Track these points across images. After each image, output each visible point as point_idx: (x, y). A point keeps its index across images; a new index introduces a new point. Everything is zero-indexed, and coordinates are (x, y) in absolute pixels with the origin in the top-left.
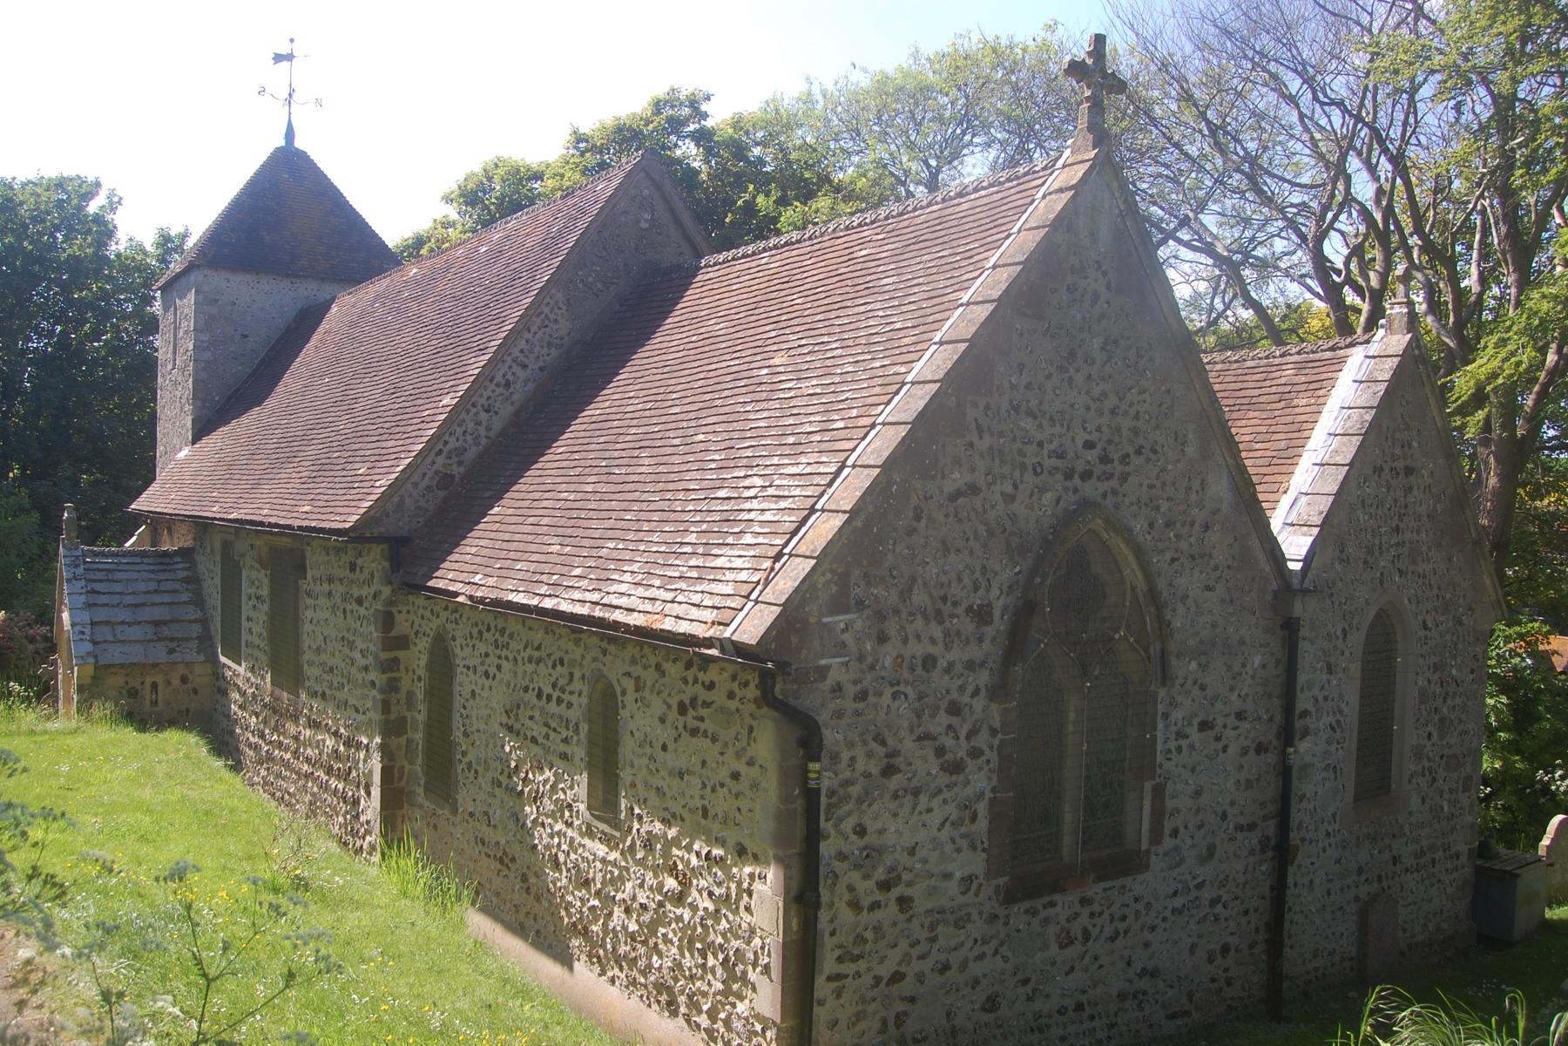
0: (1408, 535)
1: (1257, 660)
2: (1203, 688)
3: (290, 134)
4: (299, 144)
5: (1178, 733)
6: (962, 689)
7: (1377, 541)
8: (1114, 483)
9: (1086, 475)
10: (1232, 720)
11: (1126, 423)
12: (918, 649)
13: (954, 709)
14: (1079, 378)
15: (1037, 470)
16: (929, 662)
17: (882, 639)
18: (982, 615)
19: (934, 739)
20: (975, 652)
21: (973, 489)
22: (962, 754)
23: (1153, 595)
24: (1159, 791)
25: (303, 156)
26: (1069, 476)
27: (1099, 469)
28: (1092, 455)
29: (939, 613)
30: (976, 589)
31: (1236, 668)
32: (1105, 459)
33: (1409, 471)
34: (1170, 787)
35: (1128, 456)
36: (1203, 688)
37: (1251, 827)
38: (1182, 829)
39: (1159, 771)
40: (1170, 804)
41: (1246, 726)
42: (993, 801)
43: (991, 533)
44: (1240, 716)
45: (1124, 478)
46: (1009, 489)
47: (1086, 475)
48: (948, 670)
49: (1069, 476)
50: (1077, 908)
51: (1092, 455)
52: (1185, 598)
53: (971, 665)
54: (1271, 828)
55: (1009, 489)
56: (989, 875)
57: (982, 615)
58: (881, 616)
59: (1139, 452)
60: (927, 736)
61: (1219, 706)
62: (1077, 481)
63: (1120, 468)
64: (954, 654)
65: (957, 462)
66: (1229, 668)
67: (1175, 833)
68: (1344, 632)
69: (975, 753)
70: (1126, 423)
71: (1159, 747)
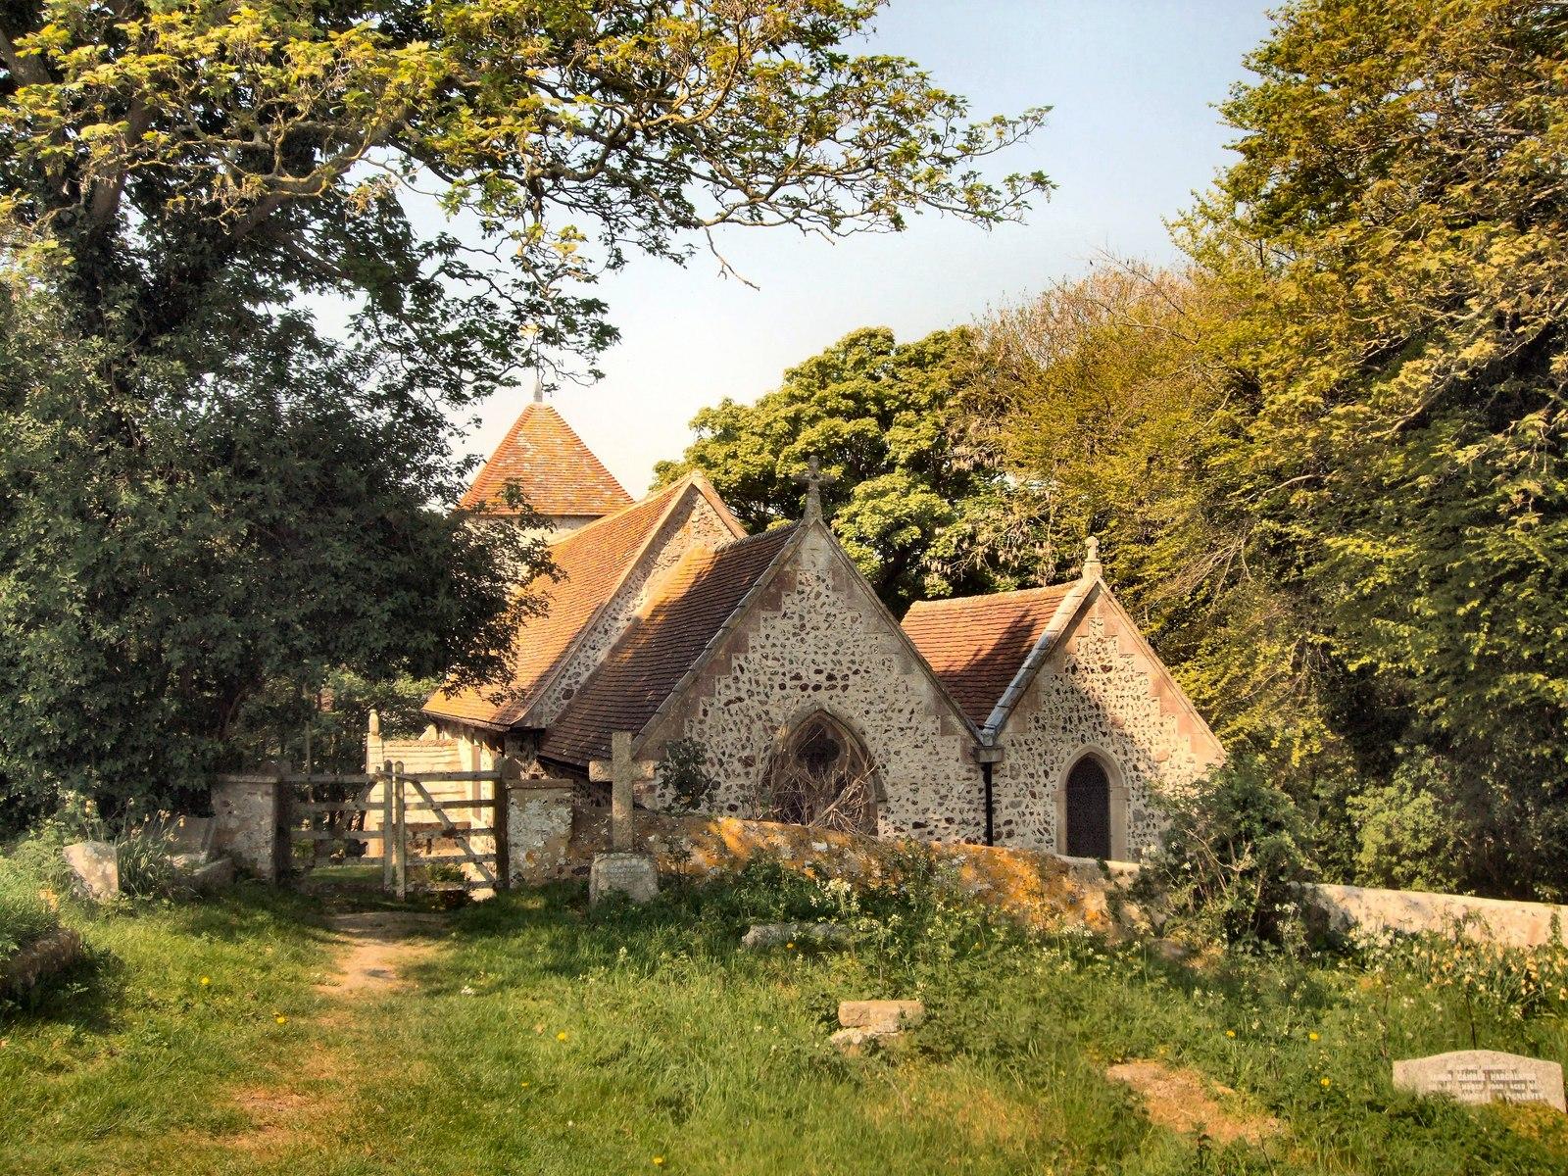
1: (961, 787)
7: (1075, 715)
8: (838, 691)
9: (817, 688)
10: (943, 824)
11: (845, 660)
14: (810, 639)
15: (783, 687)
18: (748, 762)
20: (742, 781)
21: (740, 700)
23: (864, 749)
26: (804, 688)
27: (827, 684)
28: (822, 678)
30: (744, 748)
31: (943, 792)
32: (830, 677)
33: (1106, 669)
41: (954, 827)
44: (949, 821)
45: (845, 688)
46: (763, 697)
47: (817, 688)
48: (728, 789)
49: (804, 688)
51: (822, 678)
53: (742, 787)
55: (763, 697)
57: (748, 762)
59: (856, 672)
61: (930, 815)
62: (810, 691)
63: (841, 683)
64: (734, 782)
65: (728, 687)
66: (936, 792)
68: (1046, 773)
70: (845, 660)
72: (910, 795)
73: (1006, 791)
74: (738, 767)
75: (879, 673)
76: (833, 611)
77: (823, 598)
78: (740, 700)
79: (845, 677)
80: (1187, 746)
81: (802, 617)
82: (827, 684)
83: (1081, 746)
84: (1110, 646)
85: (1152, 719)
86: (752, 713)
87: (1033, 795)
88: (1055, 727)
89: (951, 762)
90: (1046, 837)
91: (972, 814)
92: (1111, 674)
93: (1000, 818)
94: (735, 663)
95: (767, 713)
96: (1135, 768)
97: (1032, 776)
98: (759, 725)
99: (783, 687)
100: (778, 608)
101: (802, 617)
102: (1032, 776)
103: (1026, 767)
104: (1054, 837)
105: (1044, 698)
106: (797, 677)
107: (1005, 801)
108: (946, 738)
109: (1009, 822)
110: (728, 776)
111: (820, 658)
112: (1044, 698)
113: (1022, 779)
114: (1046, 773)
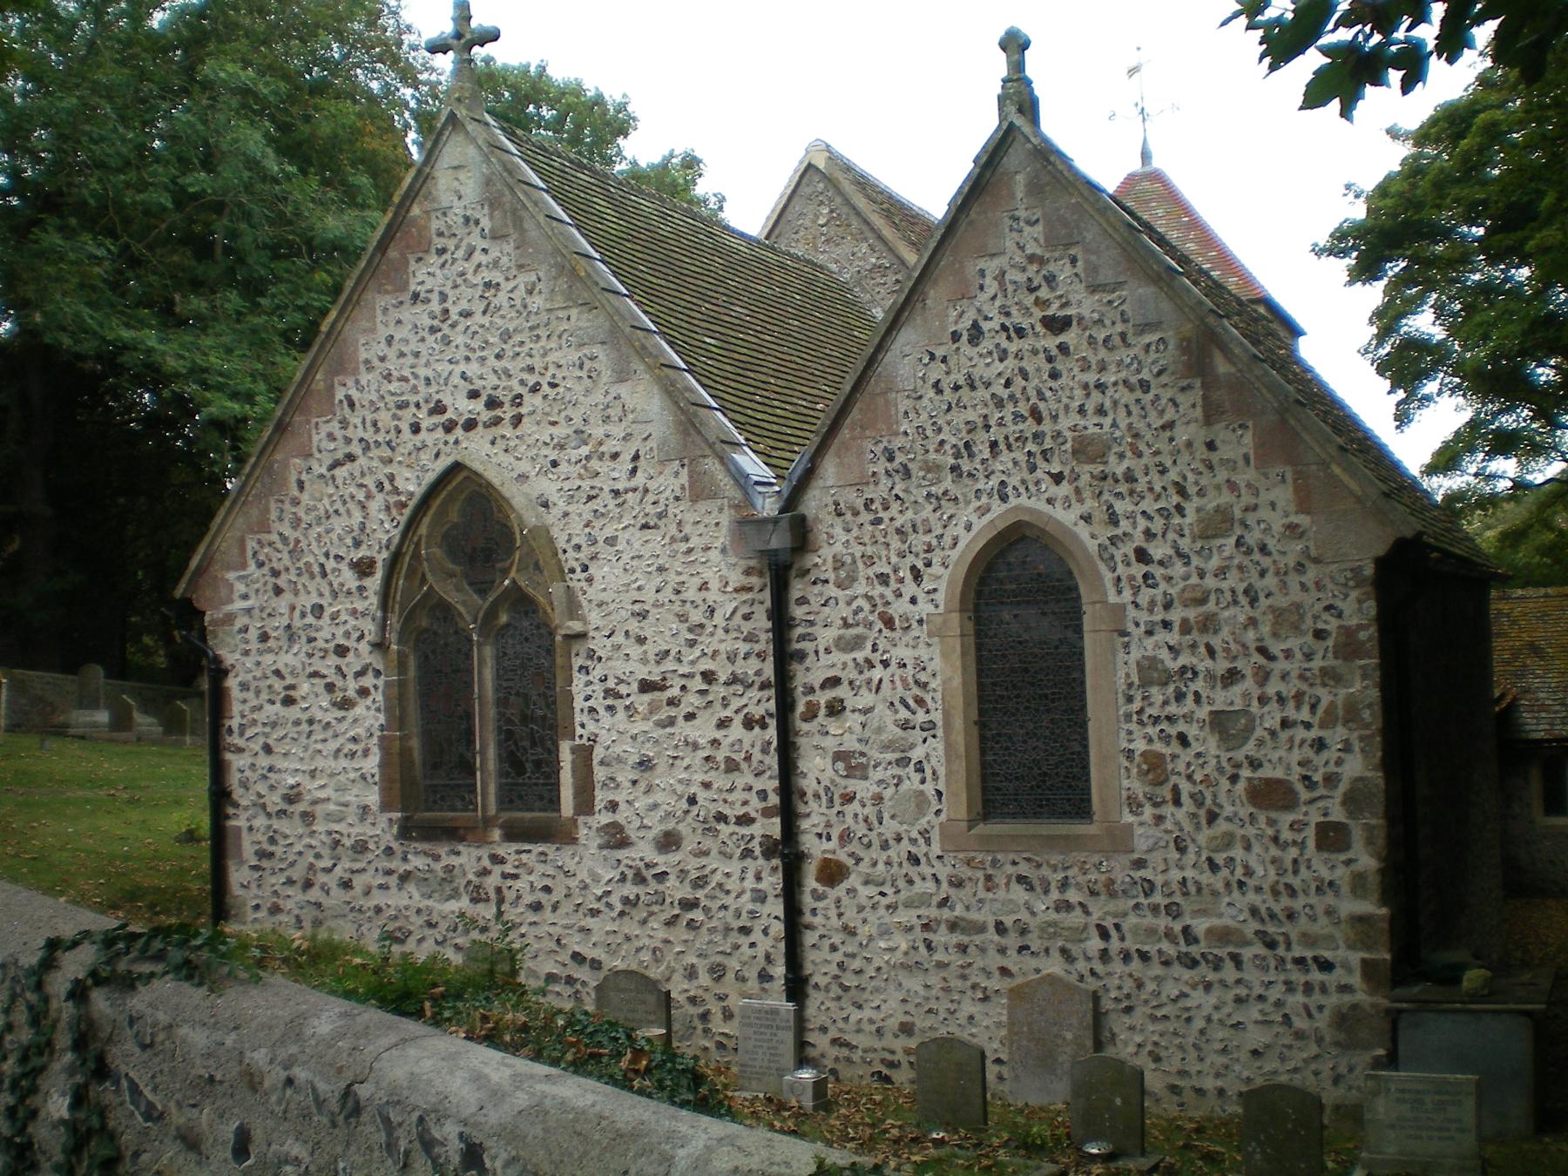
0: (1064, 423)
2: (641, 640)
3: (1146, 156)
4: (1157, 163)
5: (608, 693)
6: (347, 635)
9: (470, 425)
10: (697, 684)
12: (307, 601)
13: (342, 651)
16: (318, 610)
17: (278, 591)
18: (363, 568)
19: (324, 677)
22: (351, 693)
24: (584, 755)
25: (1157, 177)
26: (449, 427)
27: (486, 416)
29: (322, 565)
30: (357, 544)
31: (696, 617)
33: (1057, 325)
34: (599, 753)
35: (520, 396)
36: (641, 640)
37: (745, 820)
38: (623, 806)
39: (579, 731)
40: (600, 774)
42: (381, 738)
43: (369, 496)
44: (708, 677)
45: (517, 420)
47: (470, 425)
49: (449, 427)
50: (486, 863)
52: (612, 541)
54: (774, 827)
55: (387, 453)
56: (386, 806)
58: (276, 573)
60: (315, 674)
62: (459, 432)
64: (343, 605)
66: (683, 618)
67: (613, 806)
68: (917, 575)
69: (363, 692)
70: (514, 366)
71: (579, 703)
72: (634, 626)
73: (825, 612)
74: (349, 578)
75: (573, 385)
76: (496, 277)
77: (478, 257)
78: (351, 458)
79: (517, 400)
80: (1283, 495)
81: (443, 297)
82: (486, 416)
83: (998, 508)
84: (1064, 272)
85: (1182, 435)
86: (370, 481)
87: (889, 622)
88: (930, 468)
89: (714, 555)
90: (921, 717)
91: (753, 664)
92: (1070, 337)
93: (808, 675)
94: (340, 394)
95: (391, 478)
96: (1142, 556)
97: (883, 579)
98: (375, 506)
99: (416, 429)
100: (404, 287)
101: (443, 297)
102: (883, 579)
103: (870, 561)
104: (937, 717)
105: (904, 404)
106: (439, 409)
107: (826, 636)
108: (702, 506)
109: (834, 682)
110: (335, 595)
111: (473, 369)
112: (904, 404)
113: (861, 588)
114: (917, 575)
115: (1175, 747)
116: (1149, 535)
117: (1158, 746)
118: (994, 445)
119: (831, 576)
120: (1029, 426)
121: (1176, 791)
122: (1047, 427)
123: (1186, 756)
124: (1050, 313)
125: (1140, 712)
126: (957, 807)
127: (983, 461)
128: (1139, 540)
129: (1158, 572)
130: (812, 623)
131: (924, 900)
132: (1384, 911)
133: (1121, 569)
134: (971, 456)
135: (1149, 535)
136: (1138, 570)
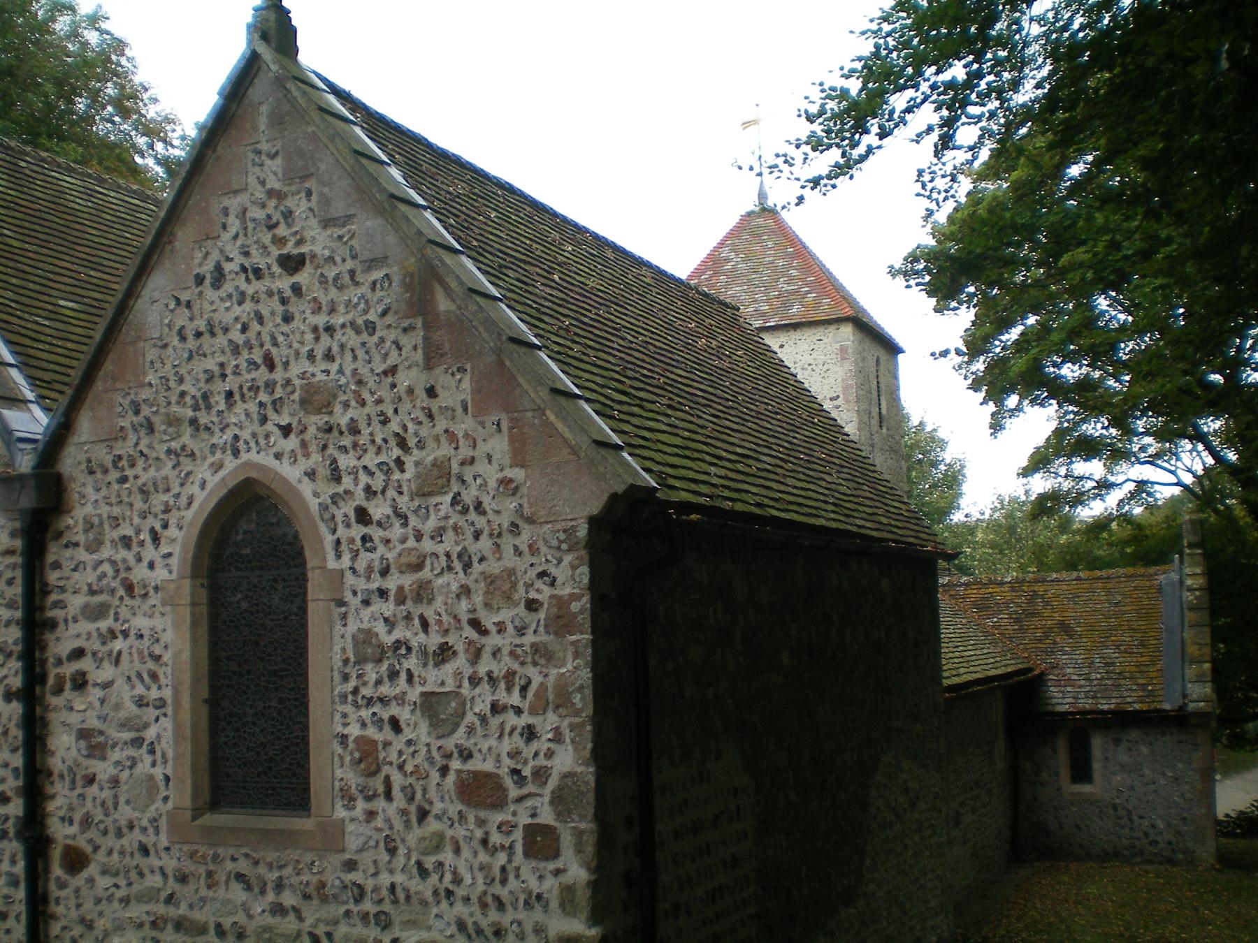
0: (295, 370)
33: (293, 264)
73: (77, 572)
80: (499, 445)
83: (230, 464)
84: (299, 205)
85: (404, 379)
87: (130, 588)
88: (173, 421)
92: (303, 277)
93: (60, 644)
96: (363, 516)
97: (126, 542)
102: (126, 542)
103: (116, 521)
104: (167, 693)
105: (152, 354)
107: (76, 602)
109: (78, 653)
112: (152, 354)
113: (106, 552)
114: (156, 538)
115: (388, 733)
116: (369, 492)
117: (371, 732)
118: (230, 394)
119: (81, 538)
120: (262, 375)
121: (388, 783)
122: (278, 375)
123: (398, 743)
124: (285, 251)
125: (356, 691)
126: (181, 796)
127: (220, 413)
128: (360, 498)
129: (377, 533)
130: (63, 589)
131: (149, 896)
132: (593, 932)
133: (341, 532)
134: (209, 407)
135: (369, 492)
136: (358, 531)
